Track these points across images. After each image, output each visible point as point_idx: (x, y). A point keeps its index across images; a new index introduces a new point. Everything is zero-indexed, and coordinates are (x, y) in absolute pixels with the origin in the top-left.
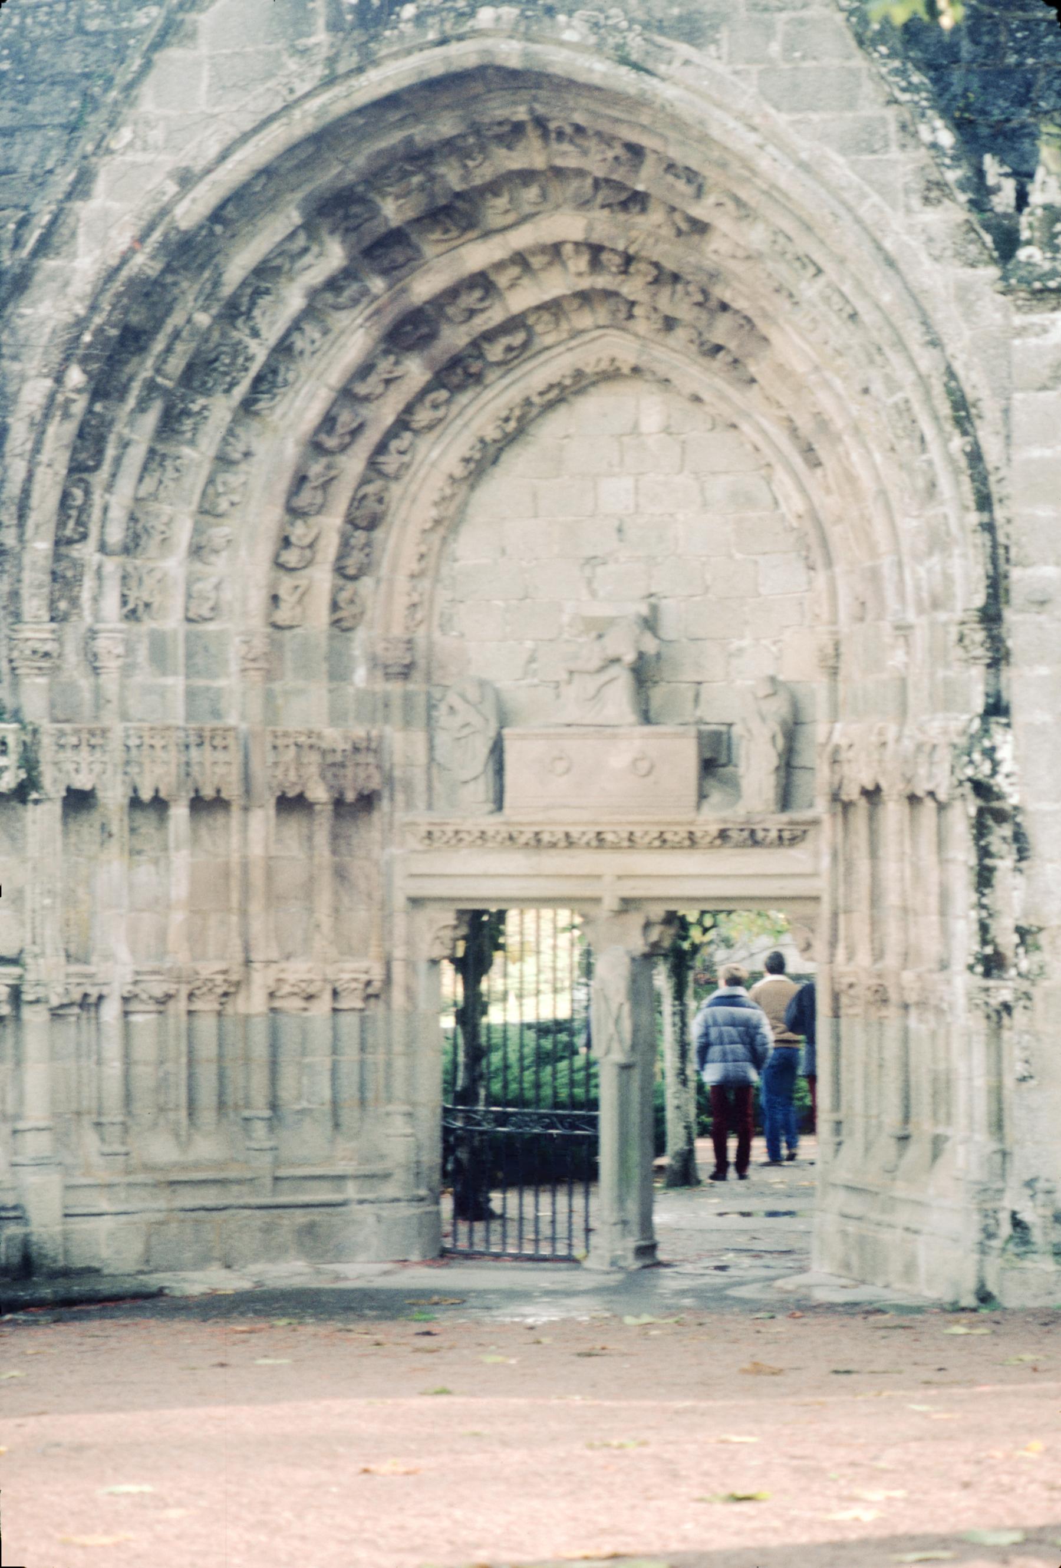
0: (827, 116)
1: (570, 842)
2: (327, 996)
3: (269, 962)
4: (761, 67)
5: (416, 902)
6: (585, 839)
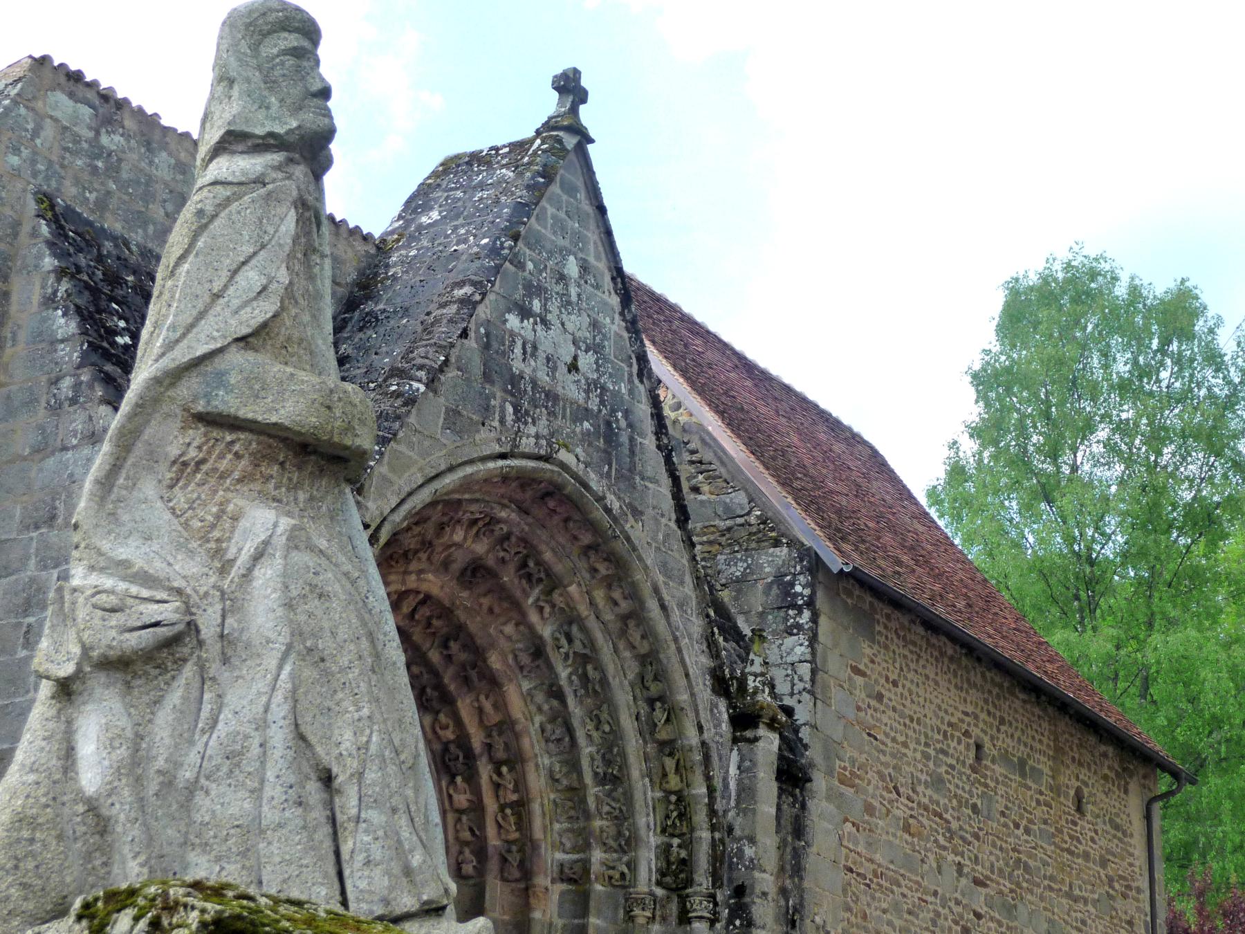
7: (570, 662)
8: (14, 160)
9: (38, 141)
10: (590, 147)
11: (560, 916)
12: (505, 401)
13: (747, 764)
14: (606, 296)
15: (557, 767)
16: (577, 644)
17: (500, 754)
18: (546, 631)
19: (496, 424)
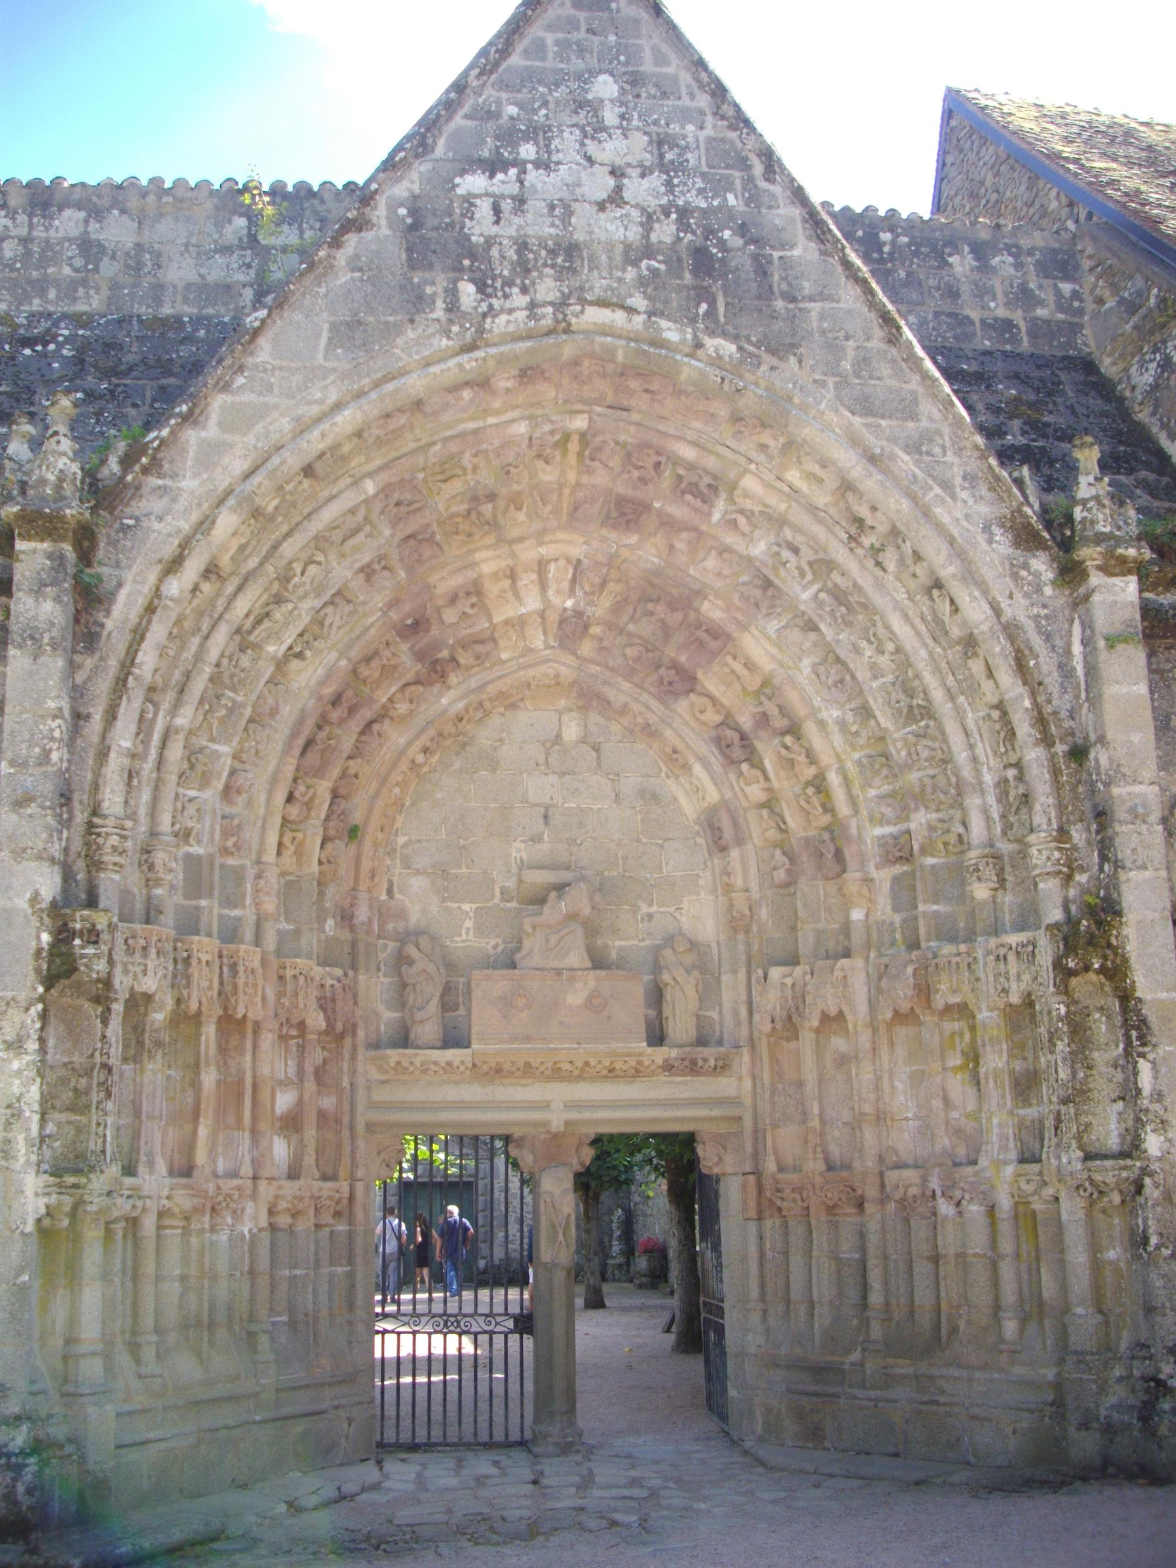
0: (894, 423)
1: (527, 1071)
2: (312, 1213)
3: (271, 1179)
4: (837, 379)
5: (370, 1128)
6: (542, 1068)
7: (809, 577)
11: (896, 909)
12: (455, 282)
13: (1088, 632)
14: (686, 101)
15: (849, 717)
16: (804, 550)
17: (780, 723)
18: (759, 549)
19: (439, 313)
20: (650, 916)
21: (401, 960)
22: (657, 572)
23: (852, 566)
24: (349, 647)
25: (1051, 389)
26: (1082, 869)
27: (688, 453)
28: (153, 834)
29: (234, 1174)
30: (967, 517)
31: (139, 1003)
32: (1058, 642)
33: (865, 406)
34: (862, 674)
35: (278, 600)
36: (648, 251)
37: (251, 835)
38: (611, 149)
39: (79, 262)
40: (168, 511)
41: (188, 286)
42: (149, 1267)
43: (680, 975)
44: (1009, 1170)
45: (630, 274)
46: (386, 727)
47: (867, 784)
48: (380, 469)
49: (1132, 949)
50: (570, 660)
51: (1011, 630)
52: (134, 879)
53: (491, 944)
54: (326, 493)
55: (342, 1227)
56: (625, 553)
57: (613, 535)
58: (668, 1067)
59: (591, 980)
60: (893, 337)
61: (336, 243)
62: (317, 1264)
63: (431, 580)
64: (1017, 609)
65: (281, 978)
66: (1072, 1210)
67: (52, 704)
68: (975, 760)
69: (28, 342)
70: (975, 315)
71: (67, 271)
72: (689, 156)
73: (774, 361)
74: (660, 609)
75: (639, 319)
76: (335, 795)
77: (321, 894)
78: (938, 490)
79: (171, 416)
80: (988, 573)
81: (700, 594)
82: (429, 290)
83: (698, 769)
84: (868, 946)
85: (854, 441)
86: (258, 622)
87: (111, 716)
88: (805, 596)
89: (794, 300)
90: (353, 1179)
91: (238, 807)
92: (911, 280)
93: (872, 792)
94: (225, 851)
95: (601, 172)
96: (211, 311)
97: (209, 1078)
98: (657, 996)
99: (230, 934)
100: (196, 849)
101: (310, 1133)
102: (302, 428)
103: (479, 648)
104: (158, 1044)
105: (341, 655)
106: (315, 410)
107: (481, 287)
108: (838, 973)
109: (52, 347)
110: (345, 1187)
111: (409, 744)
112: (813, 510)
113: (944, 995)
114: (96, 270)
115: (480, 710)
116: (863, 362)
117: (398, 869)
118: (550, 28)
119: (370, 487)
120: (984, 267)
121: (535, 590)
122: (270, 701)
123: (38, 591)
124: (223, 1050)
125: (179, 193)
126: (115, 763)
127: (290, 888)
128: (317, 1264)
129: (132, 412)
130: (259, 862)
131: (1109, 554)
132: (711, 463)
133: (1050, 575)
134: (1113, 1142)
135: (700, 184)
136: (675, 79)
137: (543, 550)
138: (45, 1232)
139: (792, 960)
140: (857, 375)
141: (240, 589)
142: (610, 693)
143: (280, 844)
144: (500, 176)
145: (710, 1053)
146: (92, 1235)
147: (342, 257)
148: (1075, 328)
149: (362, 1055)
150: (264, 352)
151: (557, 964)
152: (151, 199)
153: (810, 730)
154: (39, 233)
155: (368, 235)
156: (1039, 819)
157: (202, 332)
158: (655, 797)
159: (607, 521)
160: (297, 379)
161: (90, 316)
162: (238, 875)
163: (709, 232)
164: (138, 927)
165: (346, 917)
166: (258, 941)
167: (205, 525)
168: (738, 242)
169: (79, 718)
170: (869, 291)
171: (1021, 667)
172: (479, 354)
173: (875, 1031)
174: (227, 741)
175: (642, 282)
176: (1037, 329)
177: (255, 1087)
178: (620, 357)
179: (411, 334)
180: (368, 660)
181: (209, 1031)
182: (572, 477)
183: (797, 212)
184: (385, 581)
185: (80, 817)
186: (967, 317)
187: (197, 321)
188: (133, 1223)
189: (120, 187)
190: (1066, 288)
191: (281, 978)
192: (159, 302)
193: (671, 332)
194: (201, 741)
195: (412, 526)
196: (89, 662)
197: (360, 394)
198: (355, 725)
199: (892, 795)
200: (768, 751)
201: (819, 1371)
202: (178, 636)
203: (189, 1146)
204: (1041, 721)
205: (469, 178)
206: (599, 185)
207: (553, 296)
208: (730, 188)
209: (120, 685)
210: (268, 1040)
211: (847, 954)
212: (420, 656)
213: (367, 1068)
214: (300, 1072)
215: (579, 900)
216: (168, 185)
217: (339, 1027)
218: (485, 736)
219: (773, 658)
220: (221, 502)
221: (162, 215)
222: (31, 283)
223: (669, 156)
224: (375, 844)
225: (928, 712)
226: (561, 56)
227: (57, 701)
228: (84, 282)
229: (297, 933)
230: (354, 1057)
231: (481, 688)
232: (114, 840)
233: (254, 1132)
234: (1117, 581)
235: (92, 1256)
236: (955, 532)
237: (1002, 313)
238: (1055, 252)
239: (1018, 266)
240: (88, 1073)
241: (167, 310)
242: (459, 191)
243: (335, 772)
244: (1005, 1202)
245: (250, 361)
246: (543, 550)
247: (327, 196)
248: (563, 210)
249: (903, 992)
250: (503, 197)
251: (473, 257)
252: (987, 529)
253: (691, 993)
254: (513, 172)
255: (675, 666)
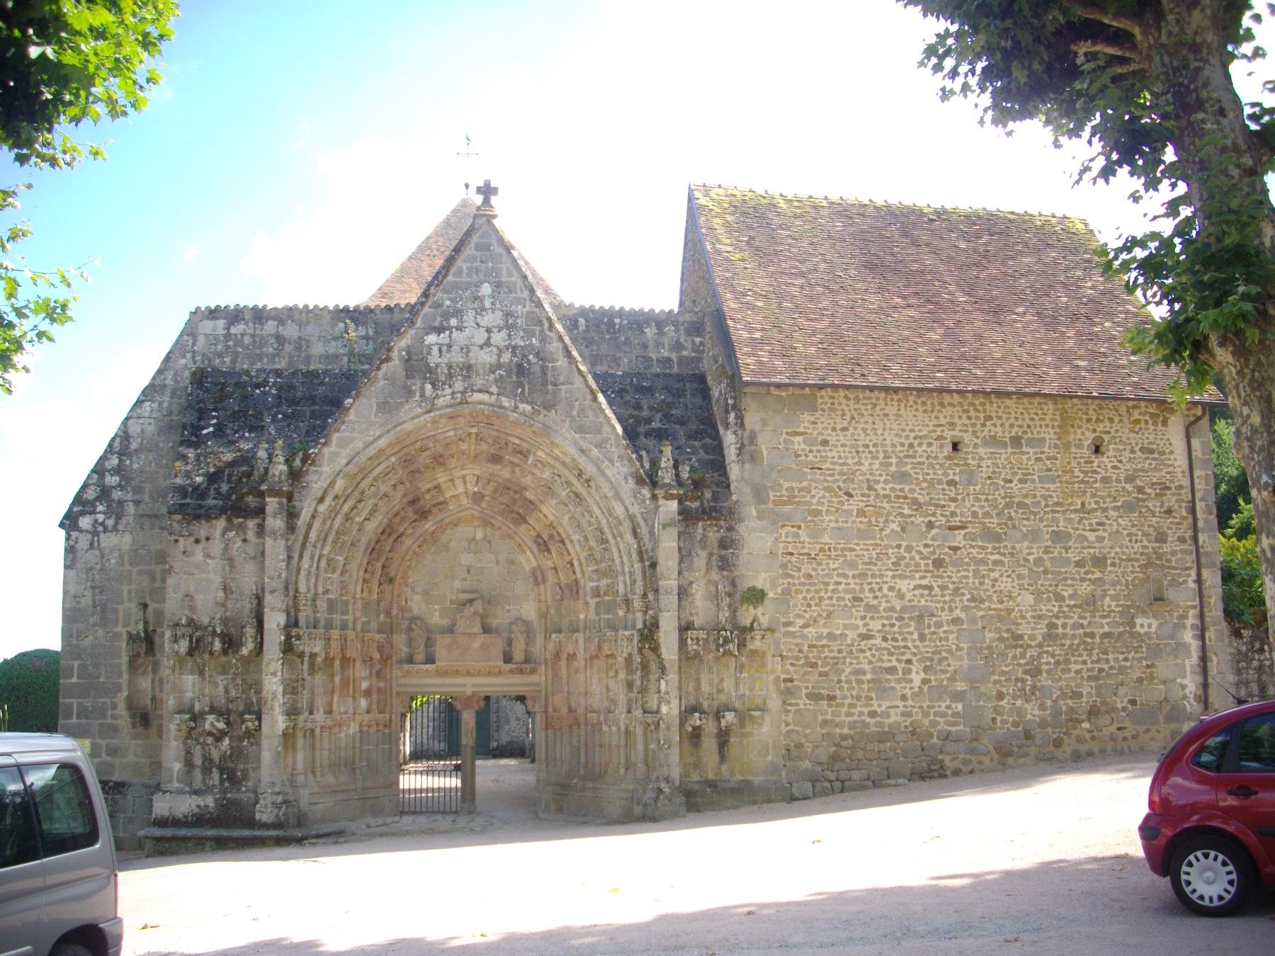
1: (457, 672)
5: (398, 694)
8: (183, 361)
9: (195, 348)
10: (494, 221)
12: (423, 384)
14: (519, 294)
15: (582, 539)
17: (558, 538)
19: (417, 398)
20: (509, 611)
21: (410, 630)
22: (508, 480)
23: (579, 486)
24: (387, 513)
25: (679, 394)
26: (651, 609)
27: (517, 441)
28: (316, 594)
29: (346, 713)
30: (618, 473)
31: (313, 656)
32: (650, 522)
33: (581, 430)
34: (585, 525)
35: (360, 501)
36: (499, 366)
37: (351, 588)
38: (488, 319)
39: (275, 346)
40: (319, 480)
41: (321, 356)
42: (318, 745)
43: (519, 635)
44: (623, 716)
45: (492, 377)
46: (404, 538)
47: (588, 566)
48: (398, 452)
49: (661, 641)
50: (477, 507)
51: (632, 518)
52: (310, 611)
53: (446, 622)
54: (376, 463)
55: (387, 731)
56: (496, 472)
57: (491, 466)
58: (511, 671)
59: (483, 638)
60: (595, 399)
61: (378, 368)
62: (377, 745)
63: (420, 485)
64: (635, 510)
65: (363, 641)
66: (639, 731)
67: (281, 557)
68: (622, 562)
69: (258, 386)
70: (654, 356)
71: (271, 350)
72: (519, 321)
73: (546, 412)
74: (511, 492)
75: (494, 397)
76: (383, 567)
77: (378, 605)
78: (607, 463)
79: (318, 443)
80: (624, 496)
81: (525, 489)
82: (414, 388)
83: (528, 552)
84: (585, 628)
85: (576, 444)
86: (353, 509)
87: (301, 557)
88: (564, 494)
89: (555, 385)
90: (391, 713)
91: (346, 578)
92: (627, 340)
93: (590, 569)
94: (341, 595)
95: (482, 330)
96: (330, 367)
97: (337, 679)
98: (510, 642)
99: (344, 626)
100: (331, 596)
101: (375, 697)
102: (367, 446)
103: (440, 507)
104: (320, 668)
105: (384, 517)
106: (371, 439)
107: (434, 386)
108: (574, 638)
109: (267, 388)
110: (388, 716)
111: (413, 544)
112: (564, 464)
113: (606, 651)
114: (283, 349)
115: (441, 528)
116: (582, 411)
117: (409, 592)
118: (465, 261)
119: (393, 459)
120: (660, 332)
121: (462, 484)
122: (358, 537)
123: (275, 516)
124: (342, 667)
125: (316, 312)
126: (303, 573)
127: (367, 604)
128: (377, 745)
129: (301, 424)
130: (354, 598)
131: (666, 492)
132: (525, 445)
133: (649, 496)
134: (655, 708)
135: (522, 334)
136: (515, 283)
137: (463, 472)
138: (285, 734)
139: (560, 631)
140: (579, 416)
141: (345, 501)
142: (493, 521)
143: (362, 590)
144: (442, 335)
145: (528, 666)
146: (300, 735)
147: (381, 374)
148: (699, 360)
149: (395, 666)
150: (352, 416)
151: (467, 631)
152: (304, 315)
153: (567, 542)
154: (258, 332)
155: (390, 364)
156: (637, 590)
157: (327, 379)
158: (513, 562)
159: (488, 461)
160: (364, 426)
161: (281, 370)
162: (346, 603)
163: (524, 356)
164: (313, 630)
165: (388, 613)
166: (354, 629)
167: (332, 484)
168: (536, 360)
169: (290, 557)
170: (586, 380)
171: (635, 534)
172: (432, 414)
173: (586, 660)
174: (342, 555)
175: (496, 381)
176: (683, 361)
177: (354, 681)
178: (486, 412)
179: (407, 407)
180: (395, 516)
181: (337, 663)
182: (473, 447)
183: (560, 345)
184: (401, 488)
185: (292, 593)
186: (650, 358)
187: (326, 372)
188: (313, 731)
189: (291, 309)
190: (697, 340)
191: (363, 641)
192: (309, 363)
193: (506, 402)
194: (333, 556)
195: (411, 469)
196: (292, 538)
197: (388, 431)
198: (391, 540)
199: (597, 571)
200: (554, 548)
201: (564, 786)
202: (324, 521)
203: (331, 703)
204: (640, 553)
205: (430, 336)
206: (481, 337)
207: (461, 389)
208: (534, 335)
209: (304, 545)
210: (358, 664)
211: (577, 631)
212: (416, 512)
213: (397, 671)
214: (371, 675)
215: (478, 606)
216: (311, 308)
217: (385, 657)
218: (444, 538)
219: (554, 515)
220: (338, 474)
221: (308, 322)
222: (258, 355)
223: (510, 321)
224: (400, 584)
225: (606, 541)
226: (469, 276)
227: (283, 556)
228: (278, 355)
229: (369, 622)
230: (391, 666)
231: (442, 520)
232: (304, 602)
233: (354, 697)
234: (670, 502)
235: (300, 742)
236: (613, 479)
237: (666, 354)
238: (694, 323)
239: (677, 331)
240: (297, 681)
241: (312, 367)
242: (426, 343)
243: (383, 559)
244: (623, 727)
245: (347, 419)
246: (463, 472)
247: (378, 312)
248: (466, 349)
249: (593, 648)
250: (443, 345)
251: (431, 372)
252: (626, 478)
253: (523, 642)
254: (447, 332)
255: (518, 513)
